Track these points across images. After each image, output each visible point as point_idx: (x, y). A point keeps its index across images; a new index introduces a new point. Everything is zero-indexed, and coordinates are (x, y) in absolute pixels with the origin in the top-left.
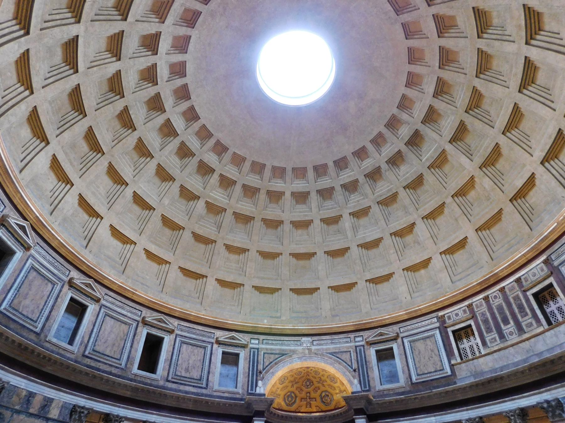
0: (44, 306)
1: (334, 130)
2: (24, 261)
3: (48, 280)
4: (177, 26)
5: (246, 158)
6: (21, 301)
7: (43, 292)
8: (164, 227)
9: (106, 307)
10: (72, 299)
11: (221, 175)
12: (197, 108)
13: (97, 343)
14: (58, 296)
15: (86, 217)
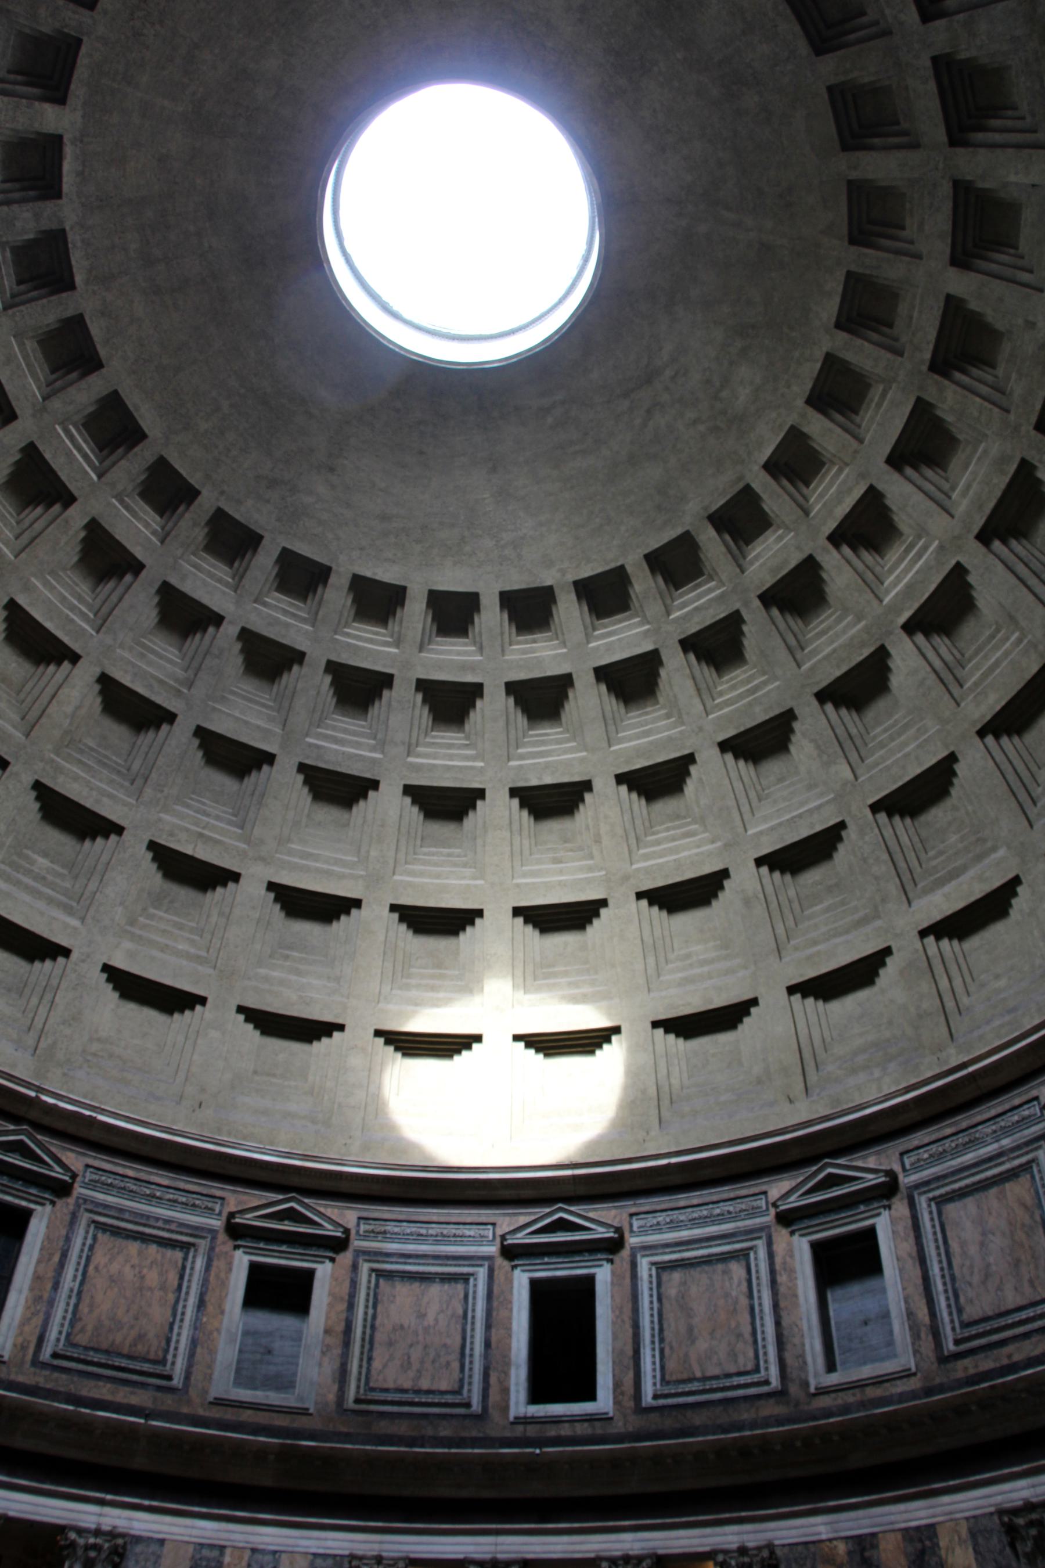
0: (753, 1324)
1: (679, 56)
2: (628, 1275)
3: (719, 1260)
4: (320, 616)
5: (792, 427)
6: (686, 1355)
7: (727, 1295)
8: (923, 818)
9: (927, 1183)
10: (819, 1249)
11: (836, 539)
12: (587, 572)
13: (962, 1300)
14: (773, 1272)
15: (724, 1039)
